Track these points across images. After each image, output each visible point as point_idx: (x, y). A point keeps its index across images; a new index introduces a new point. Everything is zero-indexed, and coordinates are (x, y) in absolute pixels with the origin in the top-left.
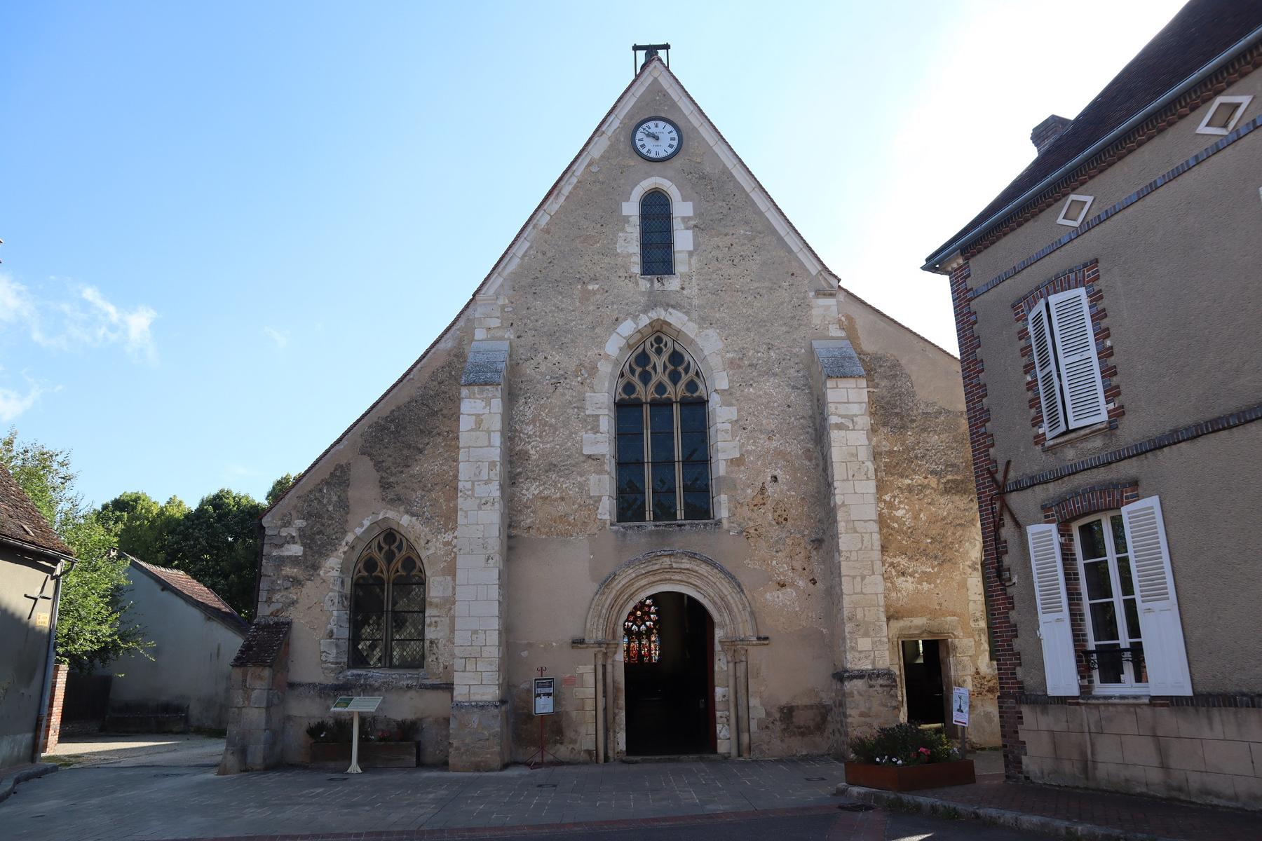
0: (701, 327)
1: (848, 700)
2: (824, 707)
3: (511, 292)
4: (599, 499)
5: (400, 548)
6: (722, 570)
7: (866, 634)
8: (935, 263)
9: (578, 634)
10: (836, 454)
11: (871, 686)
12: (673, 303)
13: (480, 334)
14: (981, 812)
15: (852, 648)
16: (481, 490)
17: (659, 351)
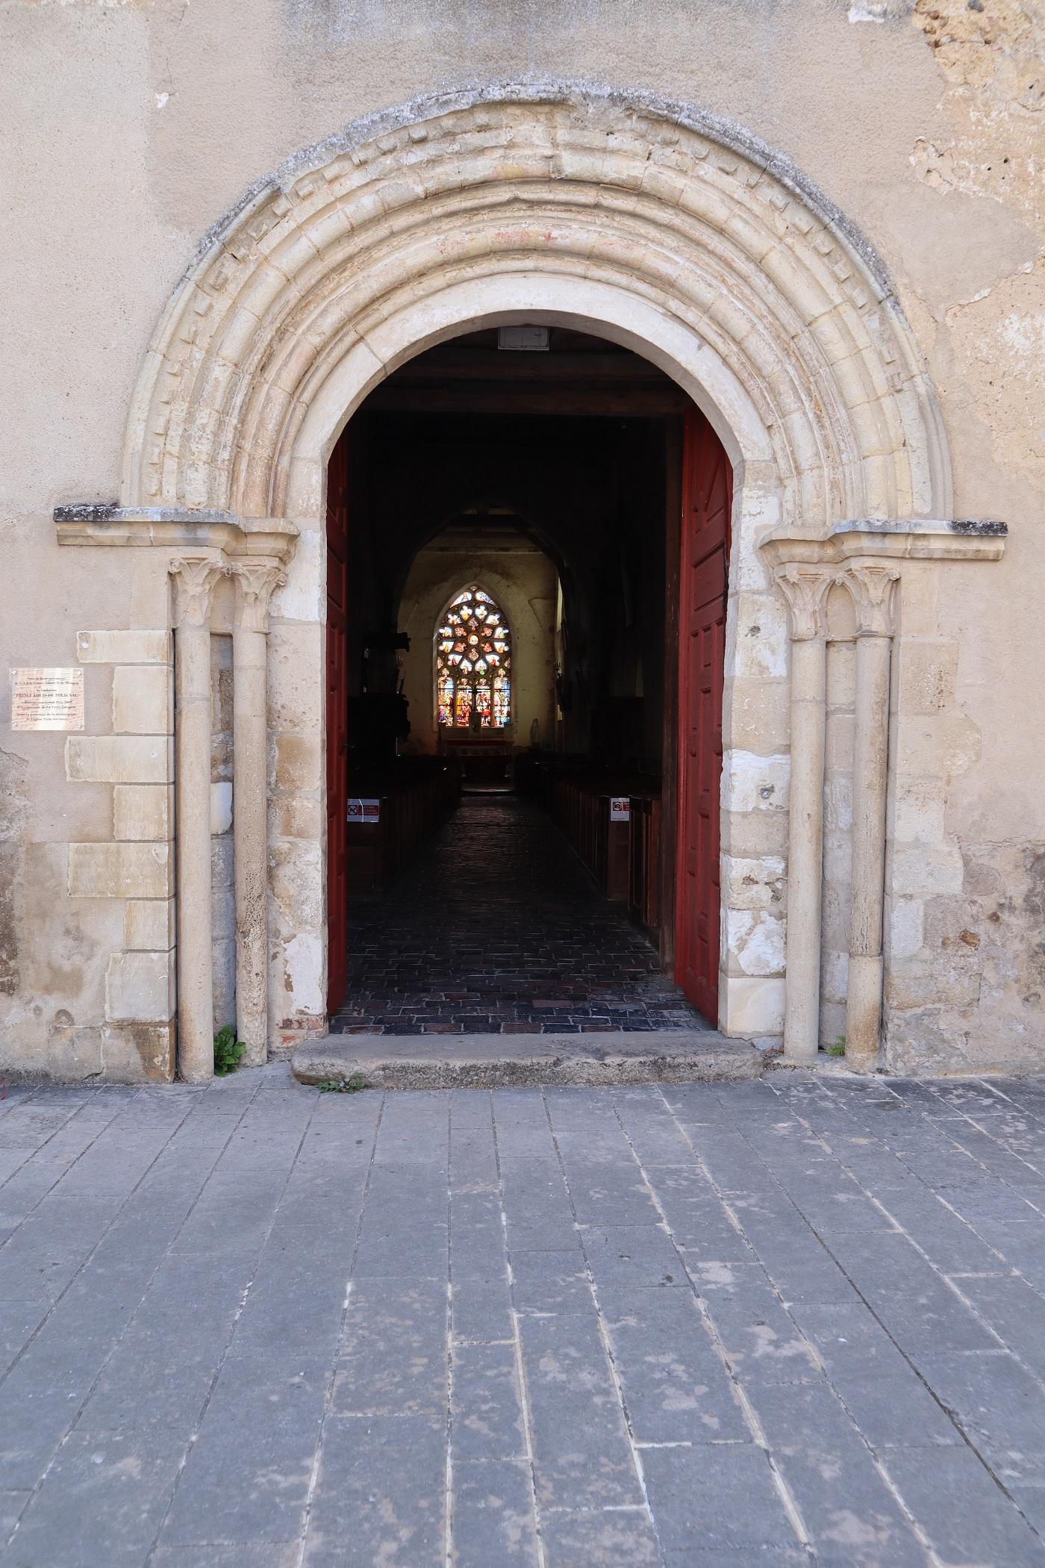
6: (800, 194)
9: (90, 485)
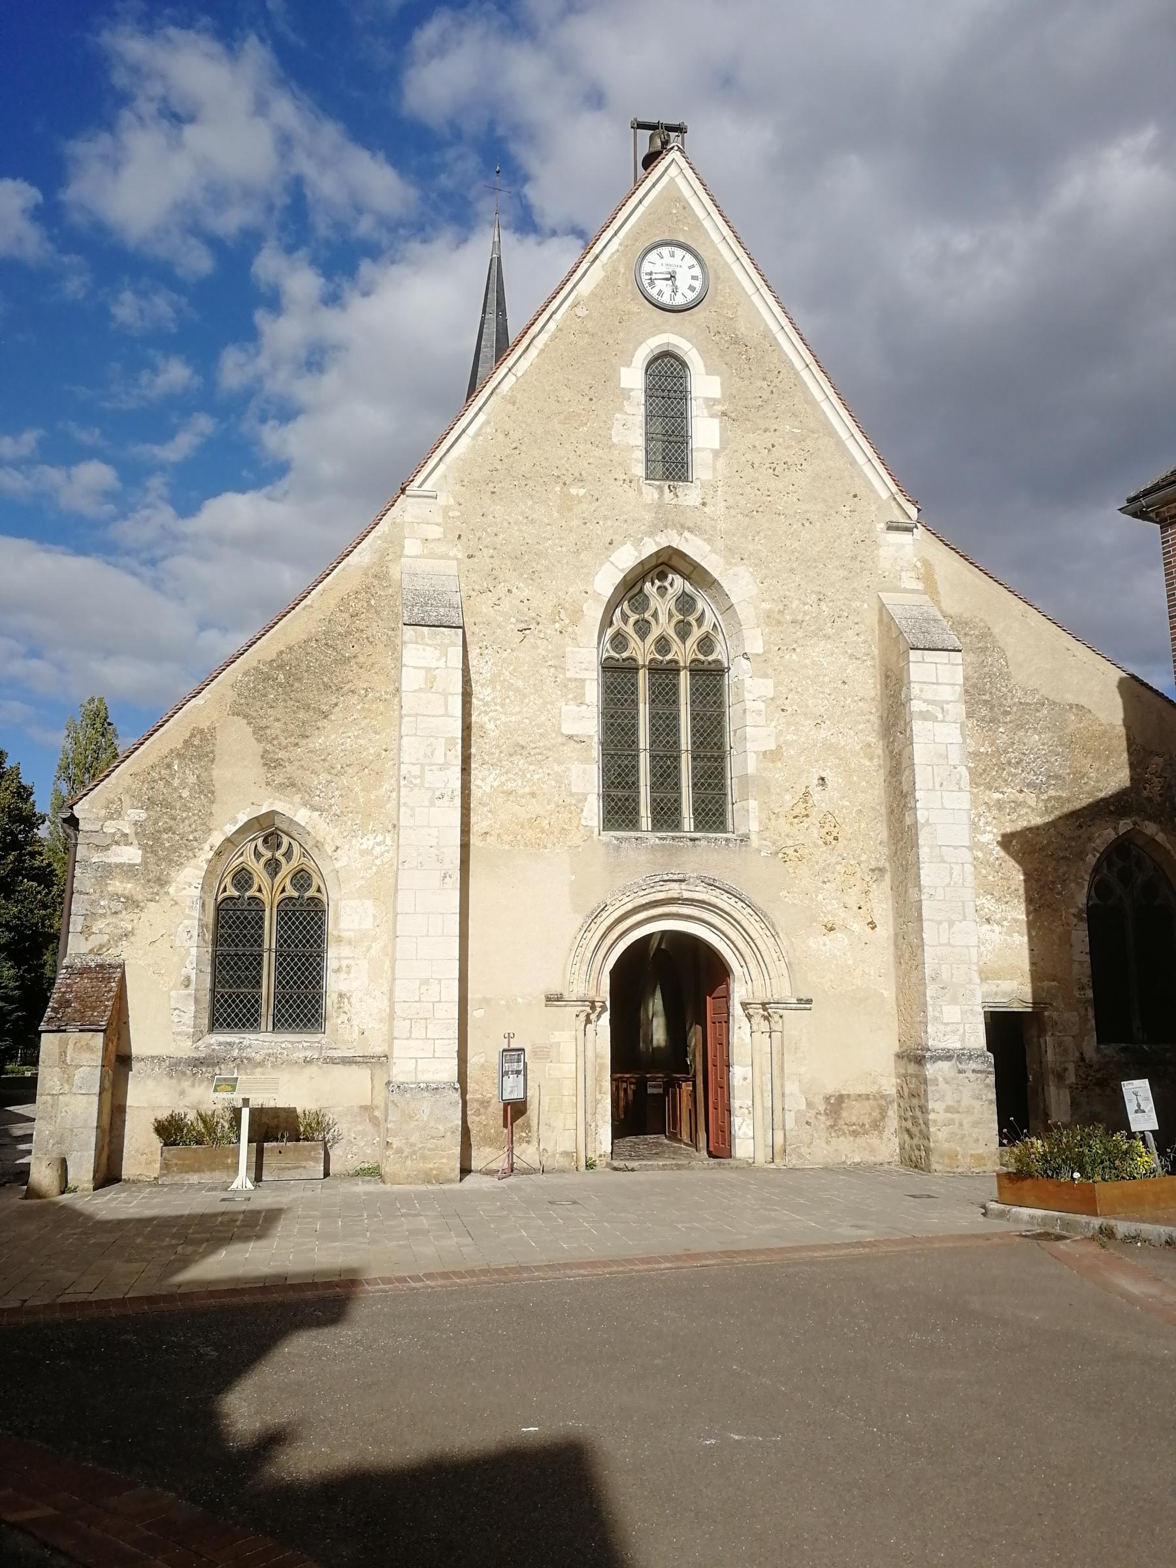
0: (728, 563)
1: (930, 1089)
2: (883, 1097)
3: (458, 487)
4: (585, 798)
7: (954, 1001)
10: (921, 754)
11: (960, 1072)
12: (690, 524)
13: (411, 547)
15: (936, 1019)
17: (662, 591)
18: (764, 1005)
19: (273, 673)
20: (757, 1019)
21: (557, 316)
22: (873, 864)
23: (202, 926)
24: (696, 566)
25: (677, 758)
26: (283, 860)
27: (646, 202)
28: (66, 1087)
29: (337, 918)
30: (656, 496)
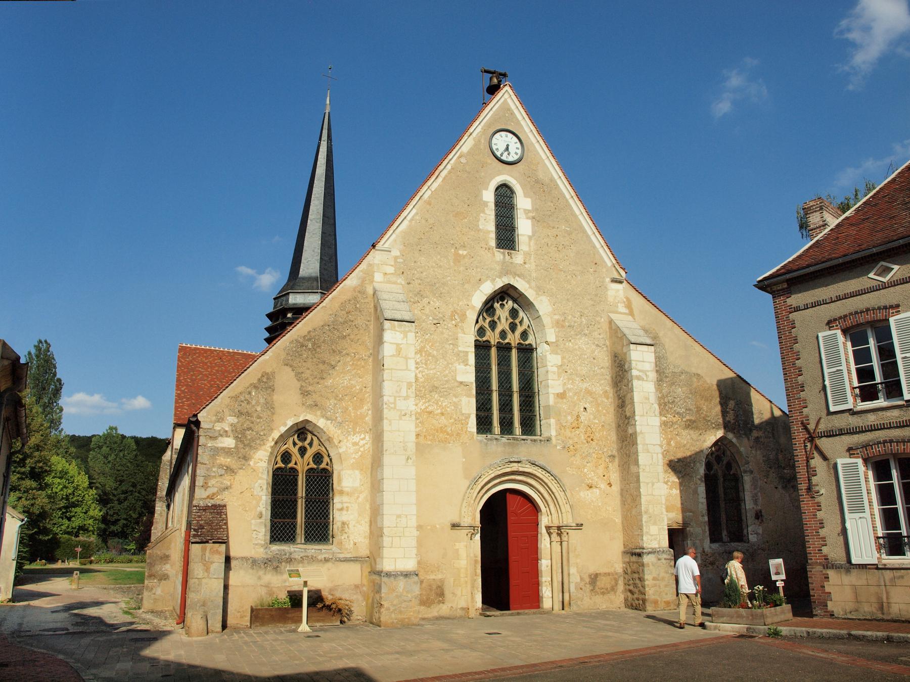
1: (646, 569)
2: (617, 574)
3: (402, 247)
4: (468, 417)
5: (311, 444)
7: (655, 524)
8: (764, 285)
9: (456, 520)
12: (518, 273)
13: (378, 277)
14: (853, 632)
15: (647, 533)
16: (401, 405)
17: (502, 306)
18: (559, 528)
19: (306, 343)
20: (554, 536)
21: (452, 162)
22: (610, 453)
23: (268, 484)
24: (521, 295)
25: (511, 396)
26: (308, 447)
27: (494, 109)
28: (206, 574)
29: (340, 481)
30: (502, 257)
